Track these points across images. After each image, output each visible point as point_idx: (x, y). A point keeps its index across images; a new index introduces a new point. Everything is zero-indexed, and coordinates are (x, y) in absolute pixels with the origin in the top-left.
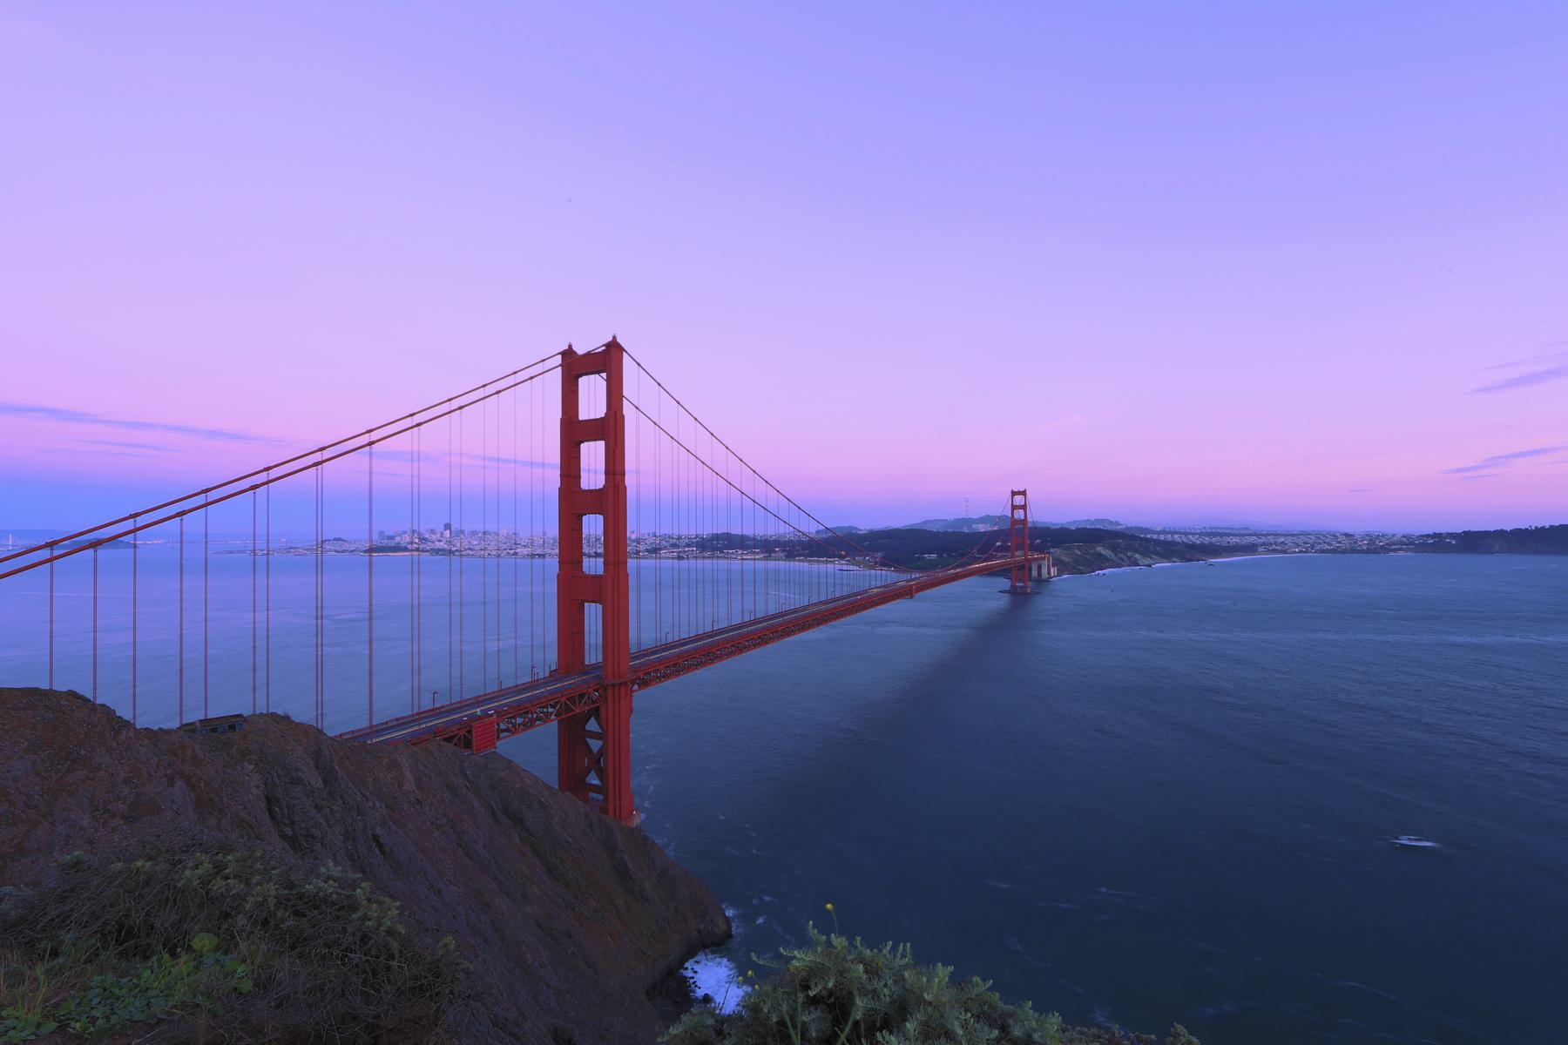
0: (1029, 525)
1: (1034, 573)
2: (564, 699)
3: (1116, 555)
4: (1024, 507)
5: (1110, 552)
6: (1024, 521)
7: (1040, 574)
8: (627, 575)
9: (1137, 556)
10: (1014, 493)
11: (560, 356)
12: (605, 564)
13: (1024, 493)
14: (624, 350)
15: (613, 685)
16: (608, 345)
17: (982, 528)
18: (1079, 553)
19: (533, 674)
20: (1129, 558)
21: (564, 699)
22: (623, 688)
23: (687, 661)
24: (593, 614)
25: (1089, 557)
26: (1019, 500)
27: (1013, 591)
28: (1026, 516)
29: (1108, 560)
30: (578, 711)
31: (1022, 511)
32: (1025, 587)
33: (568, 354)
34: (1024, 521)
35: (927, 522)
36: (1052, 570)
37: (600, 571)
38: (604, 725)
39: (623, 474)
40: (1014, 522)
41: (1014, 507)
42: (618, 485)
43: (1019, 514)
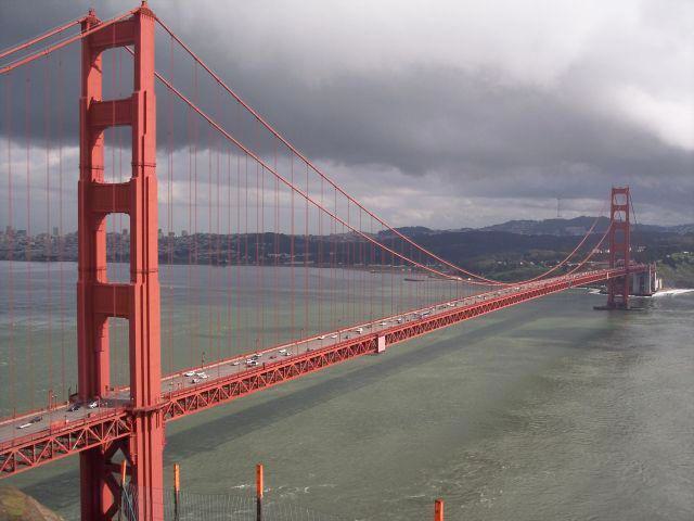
2: (86, 428)
10: (615, 191)
12: (133, 272)
13: (624, 191)
15: (143, 414)
16: (137, 15)
22: (154, 420)
26: (620, 200)
35: (513, 222)
36: (657, 282)
38: (133, 459)
40: (616, 225)
43: (620, 216)
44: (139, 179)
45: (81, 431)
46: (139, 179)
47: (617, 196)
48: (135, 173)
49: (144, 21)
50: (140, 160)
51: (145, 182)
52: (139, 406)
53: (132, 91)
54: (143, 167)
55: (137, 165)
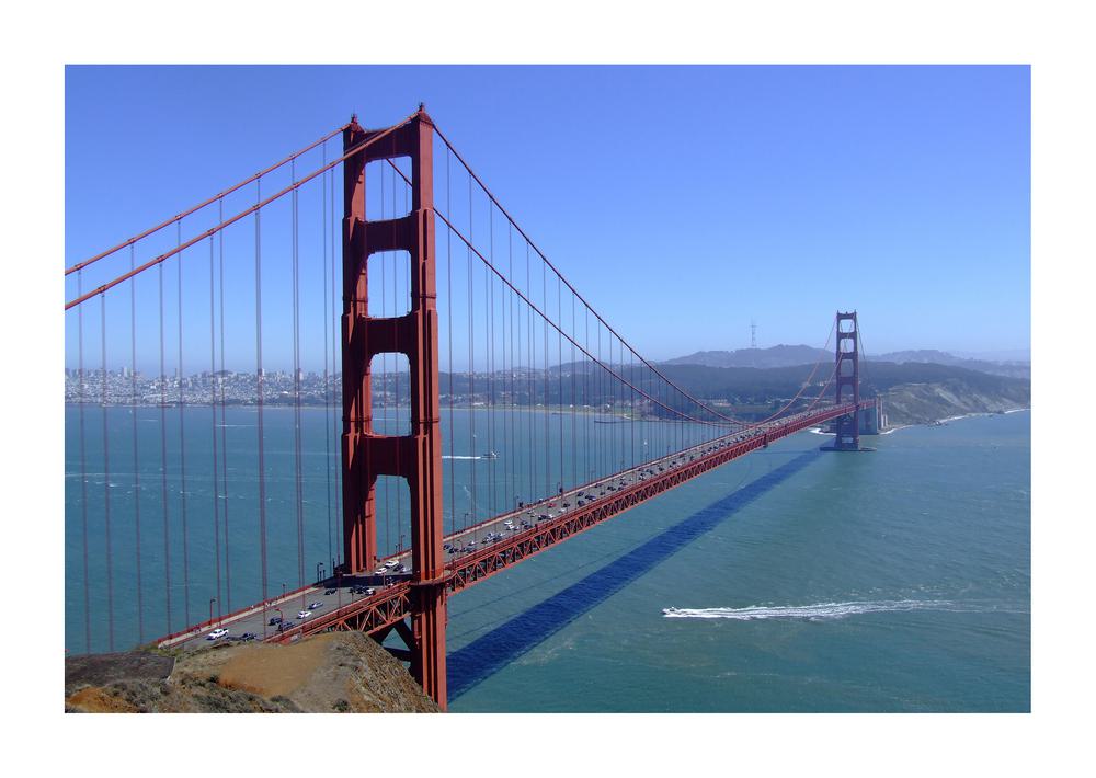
0: (860, 359)
1: (861, 424)
3: (959, 397)
4: (853, 336)
5: (951, 395)
6: (853, 355)
7: (867, 426)
8: (440, 435)
9: (984, 399)
10: (840, 317)
11: (342, 133)
13: (852, 316)
14: (434, 127)
17: (775, 364)
18: (913, 396)
19: (319, 573)
20: (975, 401)
21: (374, 608)
23: (504, 552)
24: (388, 493)
25: (925, 401)
26: (846, 326)
27: (839, 447)
28: (855, 348)
29: (949, 405)
30: (389, 623)
31: (851, 341)
32: (855, 443)
33: (353, 135)
34: (853, 355)
35: (701, 354)
37: (405, 429)
39: (434, 298)
40: (840, 355)
41: (841, 336)
42: (430, 311)
43: (847, 345)
44: (420, 313)
45: (366, 612)
46: (420, 313)
47: (842, 321)
48: (415, 306)
49: (423, 128)
50: (421, 292)
51: (428, 317)
52: (423, 582)
53: (410, 209)
54: (425, 297)
55: (420, 294)
